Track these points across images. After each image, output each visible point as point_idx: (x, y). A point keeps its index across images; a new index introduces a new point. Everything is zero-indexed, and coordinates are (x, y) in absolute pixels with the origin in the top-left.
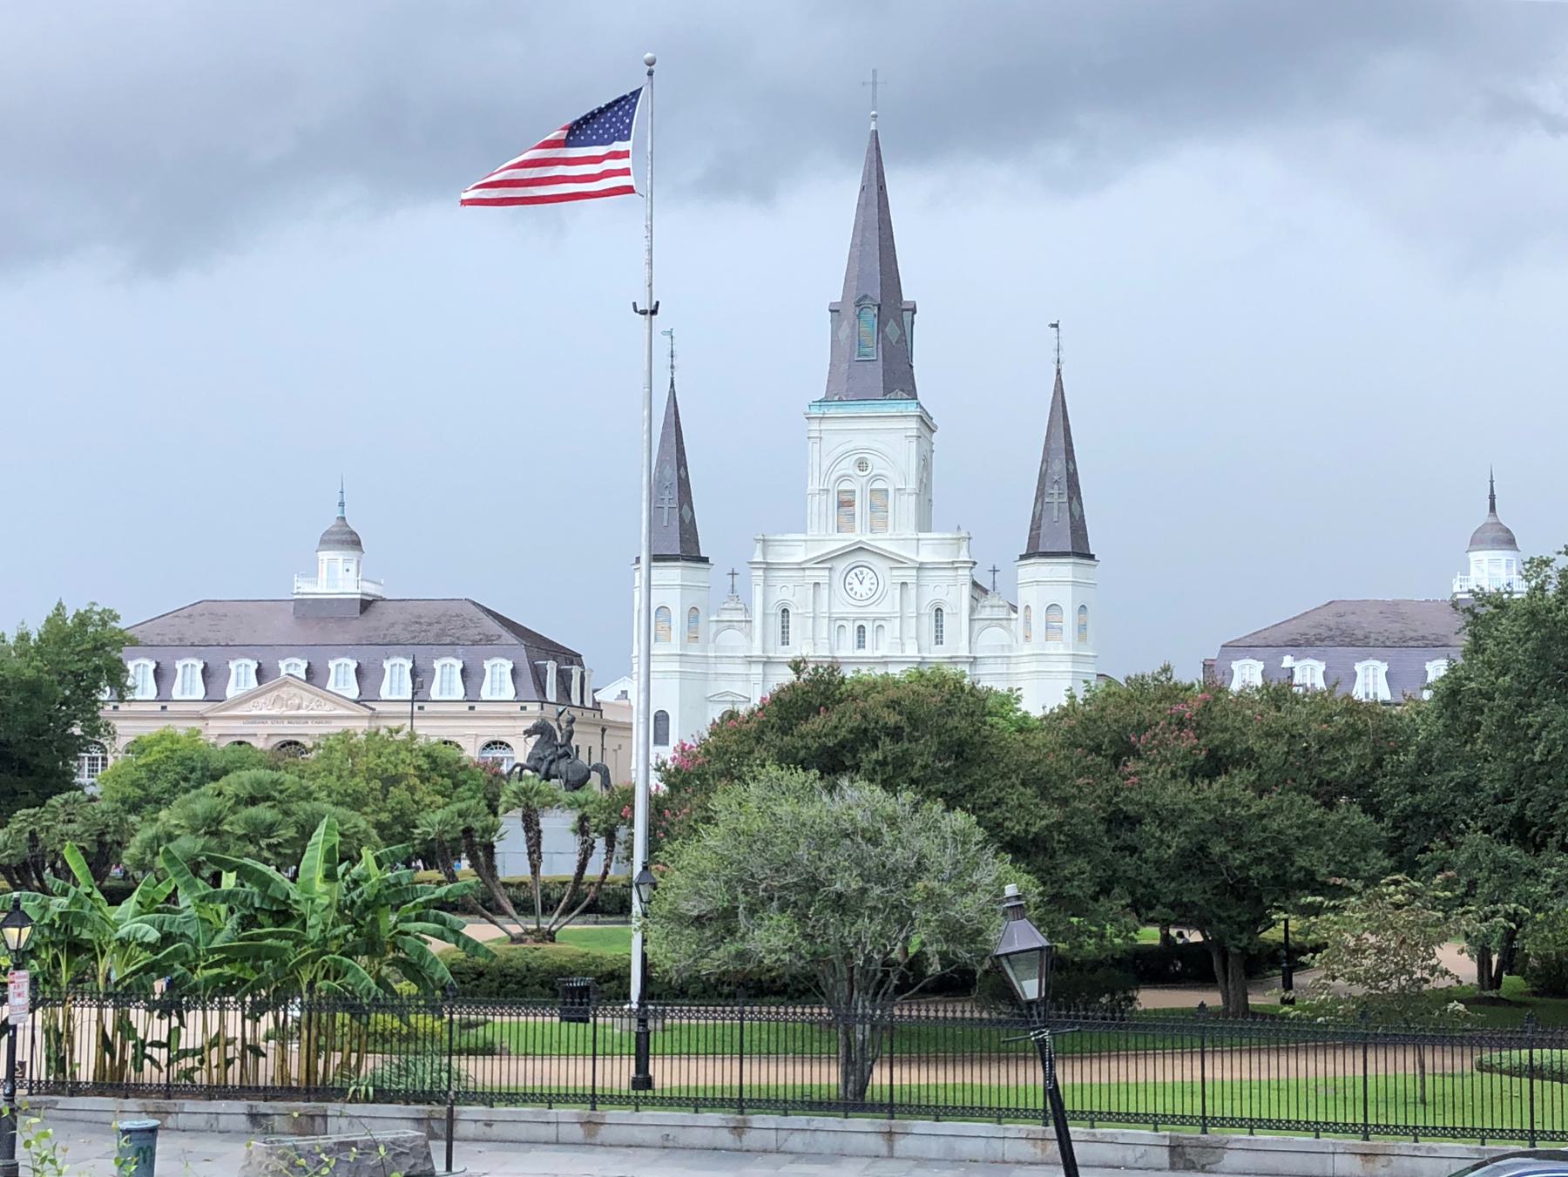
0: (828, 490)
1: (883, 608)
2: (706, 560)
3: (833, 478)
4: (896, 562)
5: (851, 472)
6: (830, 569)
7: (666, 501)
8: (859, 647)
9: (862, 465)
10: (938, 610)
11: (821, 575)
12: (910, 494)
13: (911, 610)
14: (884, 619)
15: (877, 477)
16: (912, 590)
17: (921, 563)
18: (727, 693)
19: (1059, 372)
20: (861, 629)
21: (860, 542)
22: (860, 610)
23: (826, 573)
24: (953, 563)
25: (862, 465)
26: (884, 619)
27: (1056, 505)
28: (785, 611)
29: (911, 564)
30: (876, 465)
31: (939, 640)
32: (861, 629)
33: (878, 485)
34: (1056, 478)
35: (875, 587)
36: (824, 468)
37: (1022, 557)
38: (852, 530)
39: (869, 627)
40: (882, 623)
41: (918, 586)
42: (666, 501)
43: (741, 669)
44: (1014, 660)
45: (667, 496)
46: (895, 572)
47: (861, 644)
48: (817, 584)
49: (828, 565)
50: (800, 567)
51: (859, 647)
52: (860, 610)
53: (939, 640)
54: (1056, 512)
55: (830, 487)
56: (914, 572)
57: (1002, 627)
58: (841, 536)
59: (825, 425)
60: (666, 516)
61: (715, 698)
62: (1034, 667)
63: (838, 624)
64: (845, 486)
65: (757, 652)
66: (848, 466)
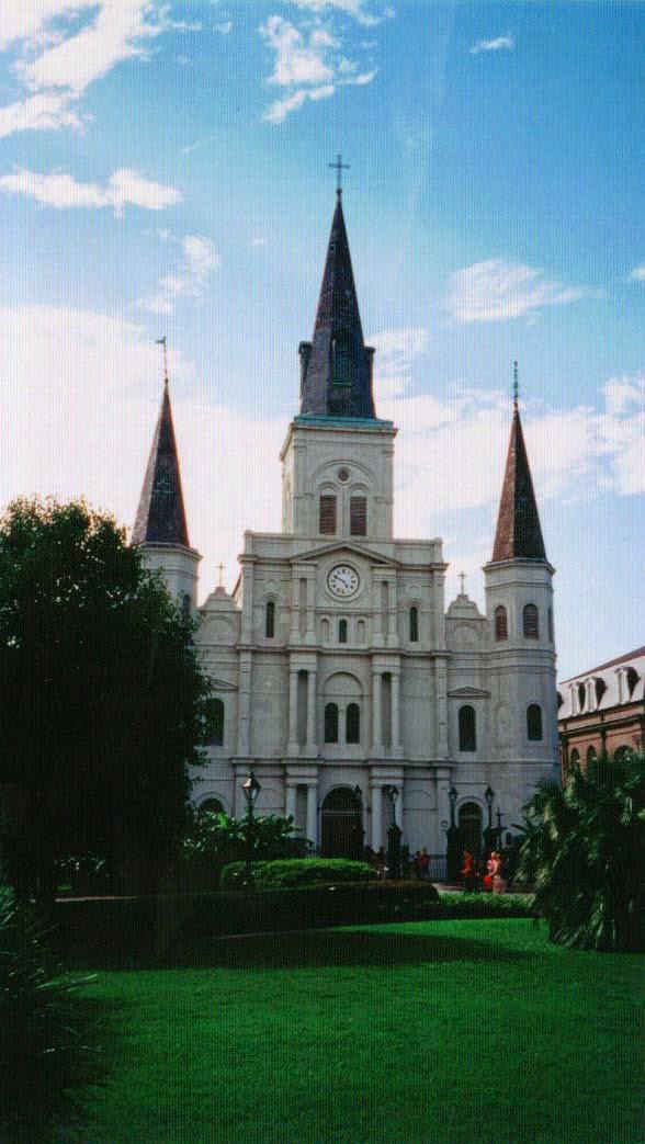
0: (312, 495)
1: (364, 605)
3: (318, 482)
4: (376, 561)
5: (332, 480)
6: (315, 565)
8: (340, 641)
9: (343, 475)
11: (307, 571)
14: (365, 615)
15: (359, 486)
16: (393, 593)
17: (401, 565)
20: (343, 625)
22: (341, 605)
23: (312, 569)
24: (430, 566)
25: (343, 475)
26: (365, 615)
28: (271, 605)
29: (392, 564)
30: (357, 475)
31: (414, 637)
32: (343, 625)
33: (358, 493)
35: (355, 585)
39: (352, 623)
40: (364, 619)
46: (376, 572)
47: (343, 638)
48: (303, 580)
49: (314, 562)
50: (288, 563)
51: (340, 641)
52: (341, 605)
53: (414, 637)
56: (394, 572)
57: (474, 628)
58: (322, 536)
59: (311, 436)
62: (514, 661)
63: (323, 616)
64: (328, 492)
65: (245, 640)
66: (331, 475)
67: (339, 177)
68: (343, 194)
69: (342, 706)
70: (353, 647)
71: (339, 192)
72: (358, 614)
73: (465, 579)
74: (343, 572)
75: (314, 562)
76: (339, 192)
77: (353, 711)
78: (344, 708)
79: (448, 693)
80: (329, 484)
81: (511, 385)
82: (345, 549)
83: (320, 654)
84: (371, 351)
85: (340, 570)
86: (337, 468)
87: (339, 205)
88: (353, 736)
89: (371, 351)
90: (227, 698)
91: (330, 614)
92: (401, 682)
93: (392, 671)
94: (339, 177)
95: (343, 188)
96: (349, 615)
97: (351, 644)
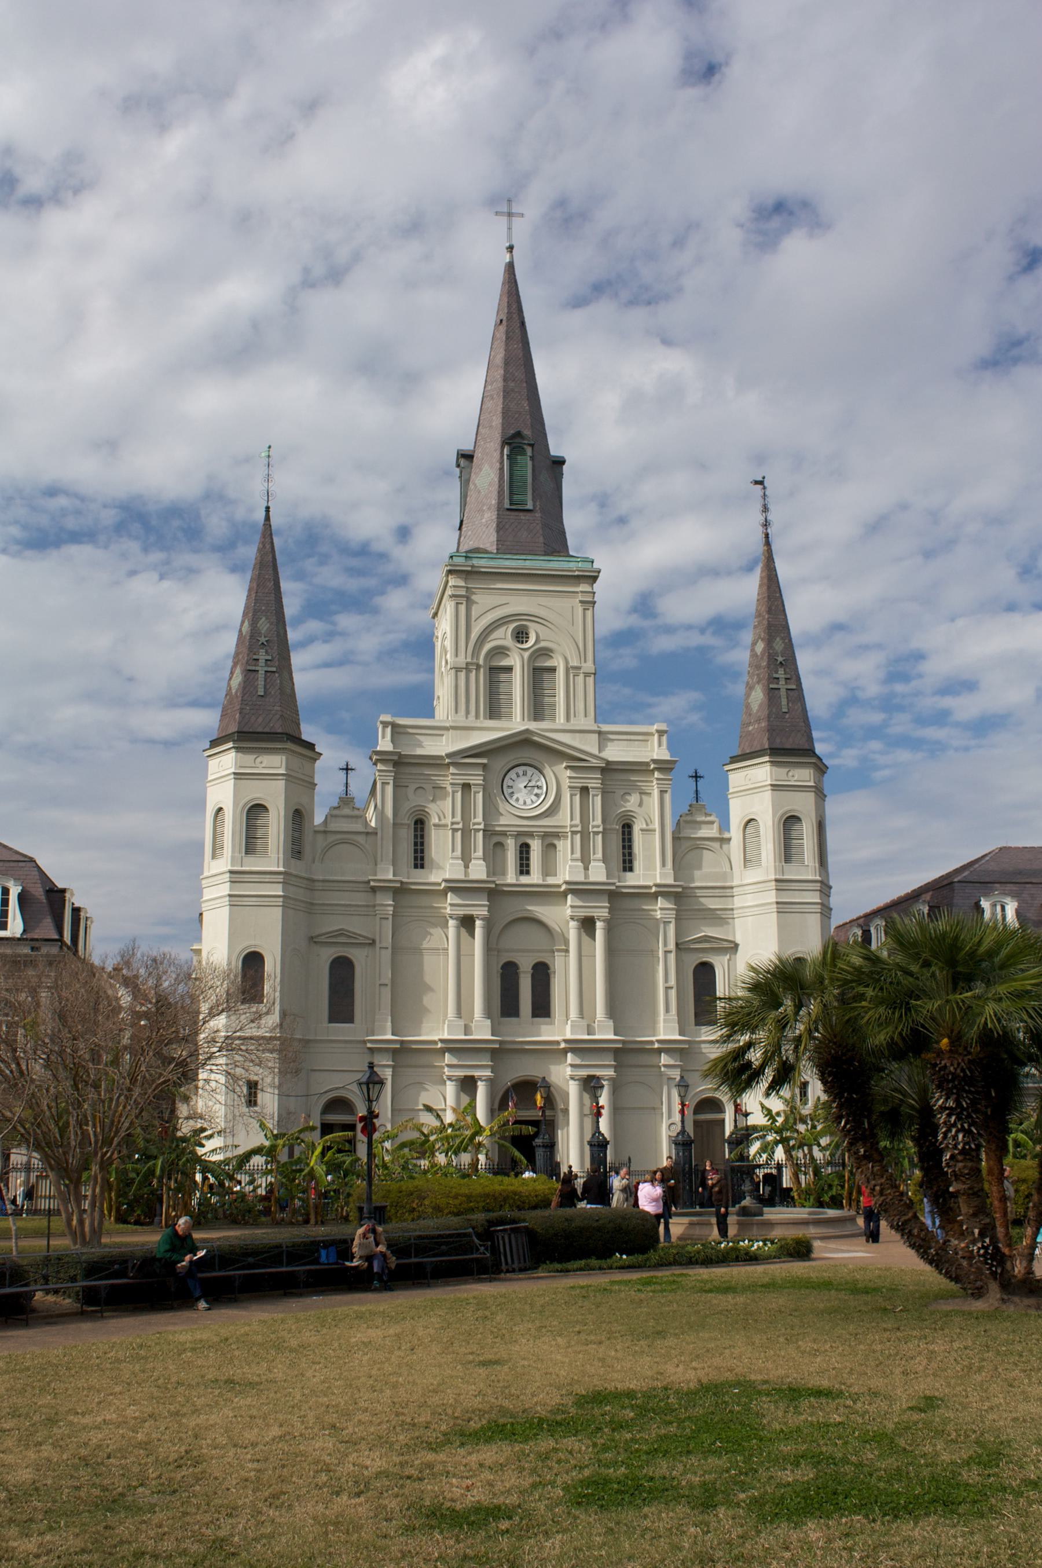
2: (311, 746)
3: (487, 647)
7: (262, 662)
9: (521, 635)
10: (623, 827)
12: (587, 675)
13: (596, 822)
17: (608, 763)
18: (341, 933)
19: (767, 536)
21: (527, 731)
25: (521, 635)
27: (783, 692)
29: (594, 762)
31: (628, 865)
34: (780, 659)
36: (474, 636)
37: (734, 759)
38: (509, 716)
39: (536, 846)
41: (605, 793)
42: (262, 662)
43: (360, 899)
44: (728, 892)
45: (262, 656)
47: (524, 868)
49: (485, 761)
51: (522, 873)
54: (784, 701)
55: (481, 662)
60: (261, 683)
61: (322, 939)
66: (504, 636)
67: (510, 229)
68: (514, 251)
69: (526, 966)
70: (541, 882)
71: (511, 248)
72: (545, 836)
73: (701, 782)
74: (525, 774)
75: (485, 761)
76: (511, 248)
77: (542, 974)
78: (530, 969)
79: (677, 944)
80: (501, 651)
81: (760, 507)
82: (523, 742)
83: (494, 893)
84: (560, 462)
85: (520, 770)
86: (512, 626)
87: (510, 267)
88: (542, 1008)
89: (560, 462)
90: (359, 957)
91: (504, 834)
92: (609, 931)
93: (595, 913)
94: (510, 229)
95: (514, 243)
96: (531, 835)
97: (535, 877)
